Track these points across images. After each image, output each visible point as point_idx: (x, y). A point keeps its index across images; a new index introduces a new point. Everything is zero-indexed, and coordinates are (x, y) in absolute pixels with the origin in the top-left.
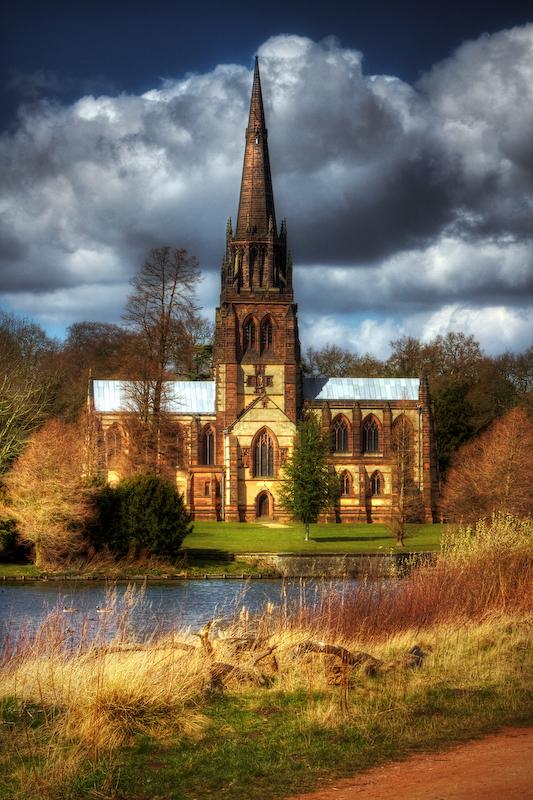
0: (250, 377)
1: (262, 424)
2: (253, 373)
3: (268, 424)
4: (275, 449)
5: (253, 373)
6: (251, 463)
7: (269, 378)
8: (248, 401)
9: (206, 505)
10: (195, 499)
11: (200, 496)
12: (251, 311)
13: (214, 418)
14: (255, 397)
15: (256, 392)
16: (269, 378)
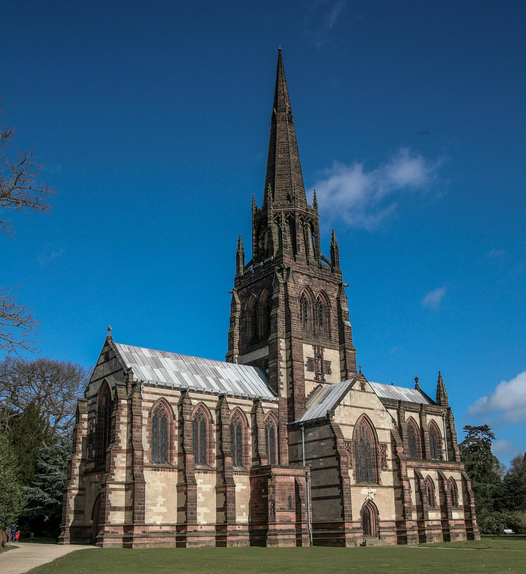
0: (310, 360)
1: (362, 411)
2: (312, 356)
3: (368, 412)
4: (372, 446)
5: (312, 356)
6: (354, 463)
7: (329, 363)
8: (309, 387)
9: (289, 522)
10: (277, 514)
11: (282, 509)
12: (306, 282)
13: (276, 406)
14: (316, 385)
15: (316, 379)
16: (329, 363)
